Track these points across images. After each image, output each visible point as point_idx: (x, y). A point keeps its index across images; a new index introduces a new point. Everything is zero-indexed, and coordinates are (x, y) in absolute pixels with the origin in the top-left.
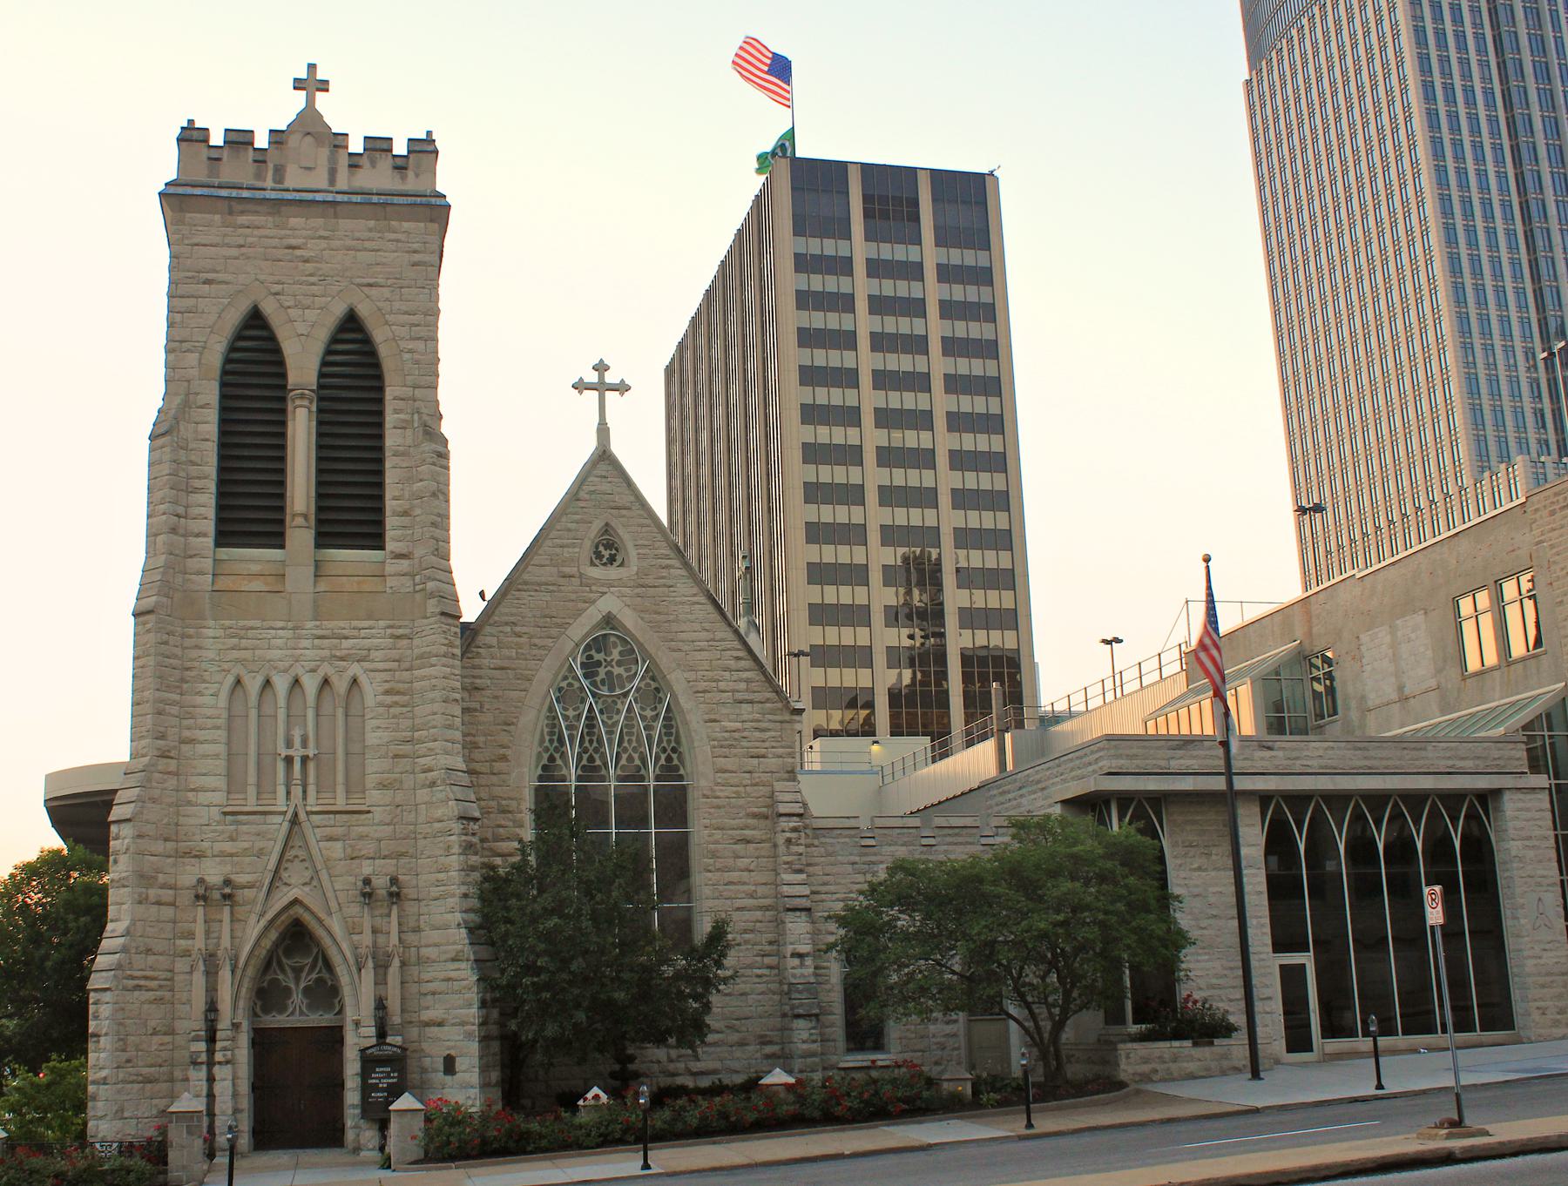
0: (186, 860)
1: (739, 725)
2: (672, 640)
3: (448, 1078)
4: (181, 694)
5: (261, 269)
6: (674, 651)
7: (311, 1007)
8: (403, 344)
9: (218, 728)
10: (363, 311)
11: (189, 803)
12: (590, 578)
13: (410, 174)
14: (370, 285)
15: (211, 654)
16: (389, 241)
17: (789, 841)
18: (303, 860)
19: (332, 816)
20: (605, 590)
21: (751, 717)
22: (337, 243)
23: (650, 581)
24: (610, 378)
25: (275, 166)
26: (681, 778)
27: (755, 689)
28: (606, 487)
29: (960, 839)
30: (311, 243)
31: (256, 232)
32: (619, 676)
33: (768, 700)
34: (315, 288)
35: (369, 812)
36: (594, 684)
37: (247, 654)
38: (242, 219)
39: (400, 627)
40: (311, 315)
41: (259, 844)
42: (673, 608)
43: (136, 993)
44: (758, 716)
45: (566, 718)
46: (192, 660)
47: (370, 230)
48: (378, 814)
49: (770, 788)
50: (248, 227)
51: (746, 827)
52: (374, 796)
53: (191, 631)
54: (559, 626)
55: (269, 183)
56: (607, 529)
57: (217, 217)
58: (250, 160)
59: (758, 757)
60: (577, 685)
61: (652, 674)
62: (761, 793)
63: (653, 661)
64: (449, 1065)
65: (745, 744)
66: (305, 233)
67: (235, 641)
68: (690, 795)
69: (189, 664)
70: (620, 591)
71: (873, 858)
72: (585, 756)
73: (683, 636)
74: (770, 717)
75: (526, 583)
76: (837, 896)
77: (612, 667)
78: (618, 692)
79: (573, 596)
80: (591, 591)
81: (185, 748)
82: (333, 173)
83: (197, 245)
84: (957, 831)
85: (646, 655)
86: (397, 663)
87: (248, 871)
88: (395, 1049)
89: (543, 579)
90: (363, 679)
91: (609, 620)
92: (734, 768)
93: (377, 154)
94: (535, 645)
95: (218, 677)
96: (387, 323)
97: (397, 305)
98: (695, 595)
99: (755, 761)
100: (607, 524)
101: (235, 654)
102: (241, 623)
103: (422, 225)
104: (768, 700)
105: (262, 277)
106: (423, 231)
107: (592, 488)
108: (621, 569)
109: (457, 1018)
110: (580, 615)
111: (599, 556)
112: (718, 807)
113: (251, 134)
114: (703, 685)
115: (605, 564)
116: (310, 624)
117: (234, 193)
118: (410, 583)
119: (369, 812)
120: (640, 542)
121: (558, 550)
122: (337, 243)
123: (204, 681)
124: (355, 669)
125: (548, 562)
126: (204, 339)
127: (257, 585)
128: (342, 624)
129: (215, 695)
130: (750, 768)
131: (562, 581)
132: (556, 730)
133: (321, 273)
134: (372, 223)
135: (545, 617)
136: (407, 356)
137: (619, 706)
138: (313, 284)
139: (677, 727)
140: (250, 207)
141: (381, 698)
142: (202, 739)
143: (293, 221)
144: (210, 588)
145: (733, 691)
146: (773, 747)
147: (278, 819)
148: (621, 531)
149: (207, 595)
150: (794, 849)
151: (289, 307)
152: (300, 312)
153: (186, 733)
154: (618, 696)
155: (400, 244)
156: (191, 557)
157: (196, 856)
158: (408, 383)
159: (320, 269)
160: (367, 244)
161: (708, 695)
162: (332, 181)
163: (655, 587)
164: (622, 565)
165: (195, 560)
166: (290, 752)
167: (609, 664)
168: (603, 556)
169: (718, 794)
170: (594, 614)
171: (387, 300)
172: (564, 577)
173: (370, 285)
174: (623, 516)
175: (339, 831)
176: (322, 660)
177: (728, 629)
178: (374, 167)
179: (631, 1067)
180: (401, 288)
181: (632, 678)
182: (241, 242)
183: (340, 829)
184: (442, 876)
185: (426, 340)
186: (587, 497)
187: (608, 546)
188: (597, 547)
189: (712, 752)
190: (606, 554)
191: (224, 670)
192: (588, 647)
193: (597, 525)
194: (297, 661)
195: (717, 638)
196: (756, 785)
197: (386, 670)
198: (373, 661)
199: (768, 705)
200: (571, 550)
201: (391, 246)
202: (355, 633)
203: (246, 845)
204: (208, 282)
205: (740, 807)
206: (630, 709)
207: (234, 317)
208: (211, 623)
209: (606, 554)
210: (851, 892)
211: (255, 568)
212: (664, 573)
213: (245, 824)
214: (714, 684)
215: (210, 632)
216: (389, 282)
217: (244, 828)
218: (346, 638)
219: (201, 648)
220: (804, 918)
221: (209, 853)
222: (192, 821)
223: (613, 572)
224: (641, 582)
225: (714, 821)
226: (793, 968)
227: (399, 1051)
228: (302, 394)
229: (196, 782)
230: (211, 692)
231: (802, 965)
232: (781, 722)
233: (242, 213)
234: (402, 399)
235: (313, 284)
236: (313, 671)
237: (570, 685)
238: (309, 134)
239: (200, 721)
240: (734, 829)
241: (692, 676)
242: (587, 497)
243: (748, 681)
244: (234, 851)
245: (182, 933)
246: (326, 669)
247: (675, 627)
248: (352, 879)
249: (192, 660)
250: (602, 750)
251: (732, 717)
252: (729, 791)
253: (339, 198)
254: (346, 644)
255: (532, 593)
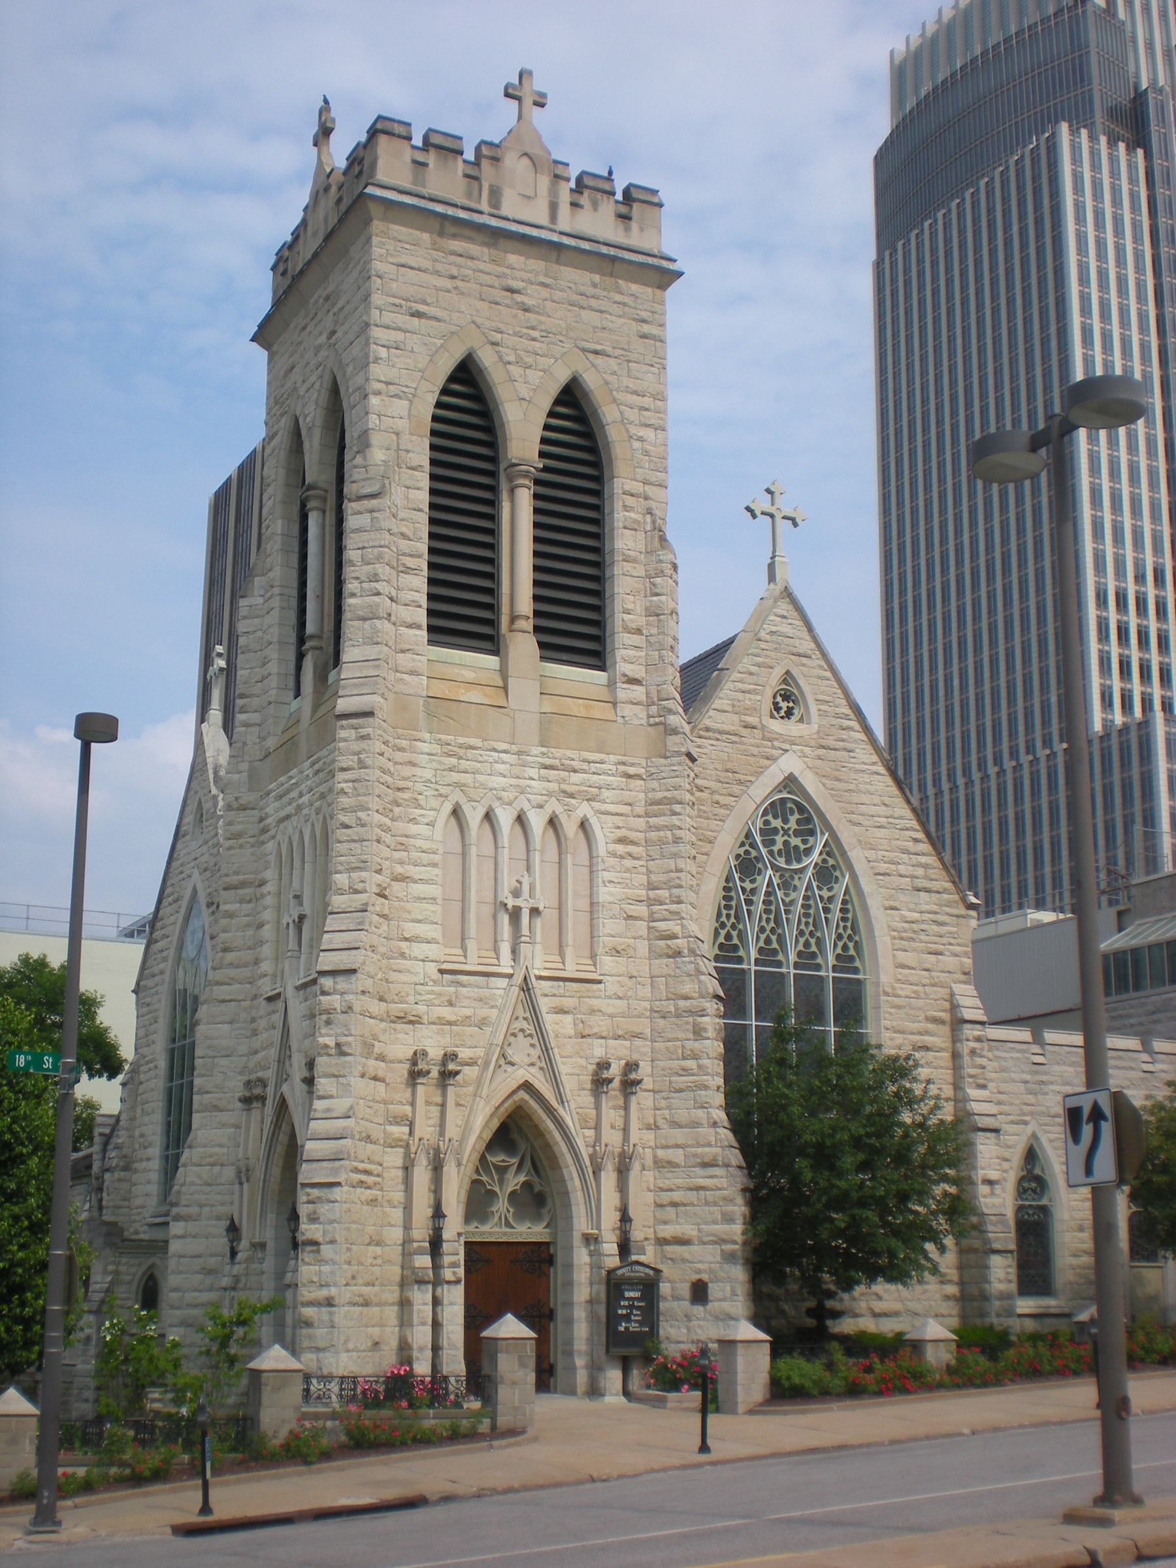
0: (399, 1026)
1: (916, 916)
2: (853, 813)
3: (698, 1309)
4: (393, 820)
5: (477, 311)
6: (855, 824)
7: (520, 1216)
8: (633, 430)
9: (435, 865)
10: (591, 380)
11: (402, 955)
12: (772, 732)
13: (634, 225)
14: (596, 352)
15: (428, 774)
16: (615, 302)
17: (973, 1052)
18: (530, 1035)
19: (561, 983)
20: (787, 747)
21: (928, 907)
22: (558, 295)
23: (830, 742)
24: (785, 506)
25: (491, 186)
26: (856, 970)
27: (933, 876)
28: (785, 629)
29: (1124, 1064)
30: (532, 289)
31: (470, 263)
32: (796, 847)
33: (945, 891)
34: (537, 345)
35: (600, 982)
36: (771, 853)
37: (467, 778)
38: (456, 245)
39: (632, 765)
40: (534, 376)
41: (483, 1012)
42: (854, 776)
43: (359, 1190)
44: (935, 908)
45: (743, 889)
46: (404, 779)
47: (595, 286)
48: (611, 985)
49: (947, 991)
50: (461, 256)
51: (927, 1033)
52: (608, 963)
53: (404, 743)
54: (740, 782)
55: (484, 206)
56: (788, 678)
57: (426, 237)
58: (460, 173)
59: (936, 954)
60: (754, 853)
61: (834, 848)
62: (940, 996)
63: (834, 835)
64: (699, 1293)
65: (923, 937)
66: (526, 276)
67: (454, 761)
68: (869, 990)
69: (402, 784)
70: (802, 752)
71: (1044, 1078)
72: (723, 932)
73: (863, 808)
74: (948, 910)
75: (707, 729)
76: (1011, 1118)
77: (789, 836)
78: (795, 866)
79: (755, 751)
80: (773, 747)
81: (397, 887)
82: (553, 207)
83: (403, 266)
84: (1121, 1053)
85: (828, 826)
86: (629, 808)
87: (469, 1043)
88: (647, 1270)
89: (726, 727)
90: (594, 822)
91: (790, 782)
92: (913, 965)
93: (599, 196)
94: (718, 803)
95: (434, 803)
96: (615, 400)
97: (626, 381)
98: (874, 764)
99: (933, 958)
100: (788, 673)
101: (455, 777)
102: (461, 740)
103: (649, 290)
104: (945, 891)
105: (479, 320)
106: (651, 298)
107: (774, 629)
108: (802, 726)
109: (712, 1235)
110: (762, 772)
111: (777, 708)
112: (899, 1007)
113: (458, 141)
114: (883, 867)
115: (782, 718)
116: (537, 750)
117: (450, 211)
118: (643, 715)
119: (600, 982)
120: (821, 697)
121: (740, 696)
122: (558, 295)
123: (420, 807)
124: (584, 809)
125: (729, 708)
126: (414, 385)
127: (475, 696)
128: (569, 753)
129: (431, 824)
130: (928, 966)
131: (744, 732)
132: (773, 908)
133: (543, 327)
134: (597, 278)
135: (727, 771)
136: (637, 445)
137: (796, 882)
138: (534, 339)
139: (854, 911)
140: (467, 232)
141: (612, 847)
142: (417, 877)
143: (513, 259)
144: (424, 693)
145: (913, 877)
146: (950, 944)
147: (502, 983)
148: (801, 682)
149: (421, 702)
150: (979, 1061)
151: (509, 363)
152: (521, 370)
153: (399, 869)
154: (796, 871)
155: (626, 309)
156: (403, 651)
157: (411, 1022)
158: (639, 477)
159: (541, 323)
160: (594, 303)
161: (887, 878)
162: (553, 217)
163: (835, 750)
164: (801, 720)
165: (409, 656)
166: (519, 902)
167: (786, 832)
168: (781, 708)
169: (900, 992)
170: (775, 775)
171: (614, 373)
172: (745, 727)
173: (596, 352)
174: (804, 665)
175: (568, 1003)
176: (550, 794)
177: (906, 806)
178: (595, 209)
179: (829, 1304)
180: (629, 361)
181: (808, 852)
182: (455, 272)
183: (570, 999)
184: (691, 1064)
185: (656, 429)
186: (768, 637)
187: (786, 698)
188: (774, 697)
189: (893, 944)
190: (784, 705)
191: (441, 795)
192: (765, 813)
193: (778, 673)
194: (522, 793)
195: (896, 815)
196: (933, 985)
197: (617, 814)
198: (604, 802)
199: (945, 896)
200: (752, 697)
201: (617, 310)
202: (585, 766)
203: (468, 1012)
204: (417, 315)
205: (920, 1009)
206: (809, 887)
207: (446, 365)
208: (427, 736)
209: (784, 705)
210: (1024, 1114)
211: (470, 675)
212: (844, 735)
213: (464, 986)
214: (893, 867)
215: (425, 747)
216: (618, 352)
217: (463, 990)
218: (575, 771)
219: (414, 765)
220: (994, 1141)
221: (425, 1019)
222: (403, 977)
223: (791, 728)
224: (823, 742)
225: (895, 1023)
226: (985, 1196)
227: (651, 1273)
228: (528, 472)
229: (411, 929)
230: (426, 821)
231: (992, 1194)
232: (957, 916)
233: (454, 236)
234: (632, 495)
235: (534, 339)
236: (541, 807)
237: (747, 852)
238: (526, 154)
239: (415, 855)
240: (913, 1033)
241: (871, 854)
242: (768, 637)
243: (926, 866)
244: (454, 1018)
245: (395, 1117)
246: (554, 806)
247: (855, 798)
248: (582, 1062)
249: (404, 779)
250: (741, 926)
251: (911, 906)
252: (907, 990)
253: (566, 241)
254: (575, 778)
255: (714, 742)
